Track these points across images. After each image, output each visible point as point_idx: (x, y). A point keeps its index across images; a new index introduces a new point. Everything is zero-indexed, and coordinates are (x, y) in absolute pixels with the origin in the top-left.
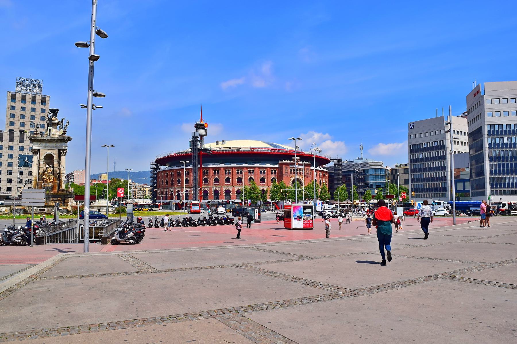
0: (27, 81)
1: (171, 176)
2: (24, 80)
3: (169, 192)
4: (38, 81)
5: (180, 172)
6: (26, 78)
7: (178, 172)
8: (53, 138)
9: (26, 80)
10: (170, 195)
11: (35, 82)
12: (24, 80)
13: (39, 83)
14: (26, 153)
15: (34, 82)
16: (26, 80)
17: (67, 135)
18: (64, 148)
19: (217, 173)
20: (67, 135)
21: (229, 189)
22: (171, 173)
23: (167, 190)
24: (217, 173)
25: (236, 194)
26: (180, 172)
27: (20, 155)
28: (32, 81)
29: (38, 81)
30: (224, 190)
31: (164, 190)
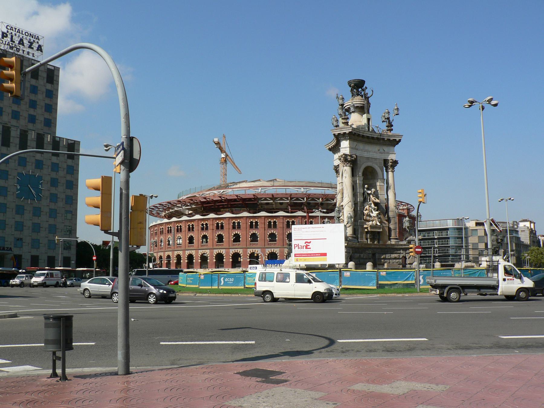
0: (20, 32)
1: (178, 231)
2: (14, 29)
3: (157, 257)
4: (36, 37)
5: (193, 225)
6: (18, 27)
7: (178, 227)
8: (381, 136)
9: (17, 30)
10: (166, 262)
11: (32, 37)
12: (14, 29)
13: (37, 40)
14: (29, 172)
15: (31, 38)
16: (17, 30)
17: (396, 131)
18: (392, 157)
19: (272, 225)
20: (396, 131)
21: (275, 252)
22: (178, 227)
23: (162, 254)
24: (272, 225)
25: (249, 260)
26: (181, 226)
27: (20, 174)
28: (27, 34)
29: (36, 37)
30: (231, 254)
31: (164, 254)
